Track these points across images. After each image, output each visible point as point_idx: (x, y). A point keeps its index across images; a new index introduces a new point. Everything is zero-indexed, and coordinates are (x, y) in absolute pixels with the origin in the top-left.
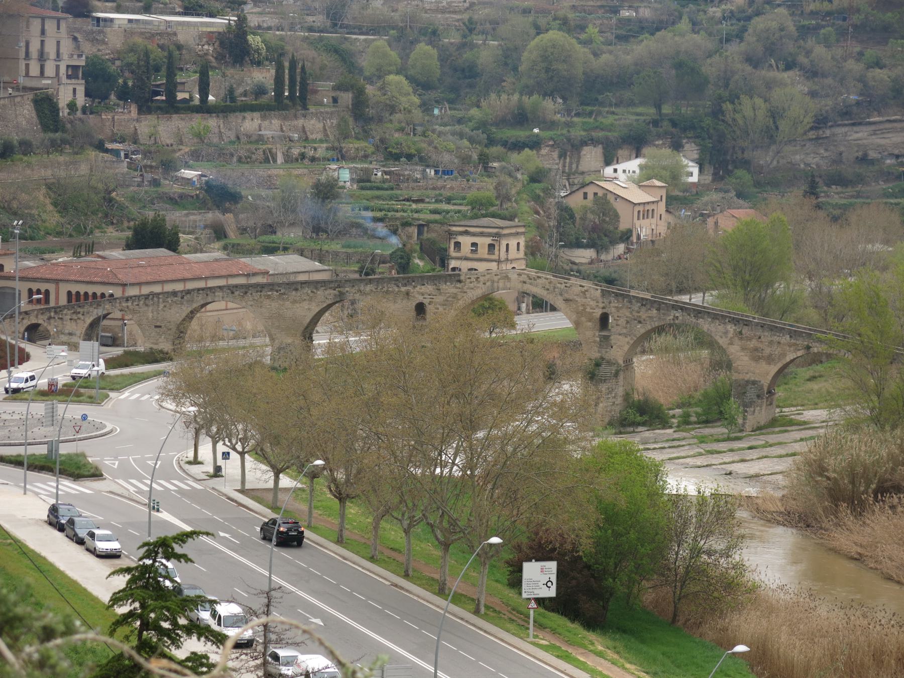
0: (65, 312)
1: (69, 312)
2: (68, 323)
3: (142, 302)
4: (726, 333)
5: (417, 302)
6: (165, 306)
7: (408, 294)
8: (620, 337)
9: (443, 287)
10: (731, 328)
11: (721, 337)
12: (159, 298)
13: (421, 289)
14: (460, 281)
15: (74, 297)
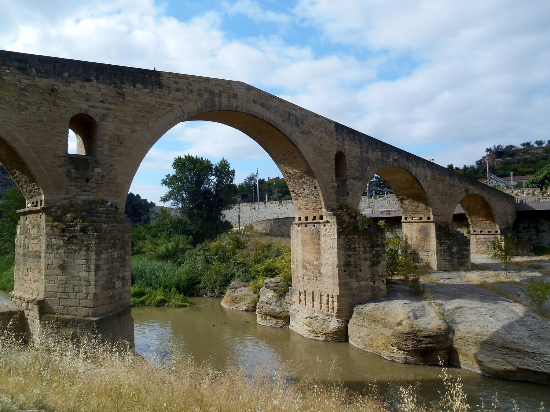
4: (426, 176)
5: (76, 112)
8: (355, 182)
9: (128, 89)
10: (428, 172)
11: (424, 182)
13: (81, 87)
14: (160, 86)
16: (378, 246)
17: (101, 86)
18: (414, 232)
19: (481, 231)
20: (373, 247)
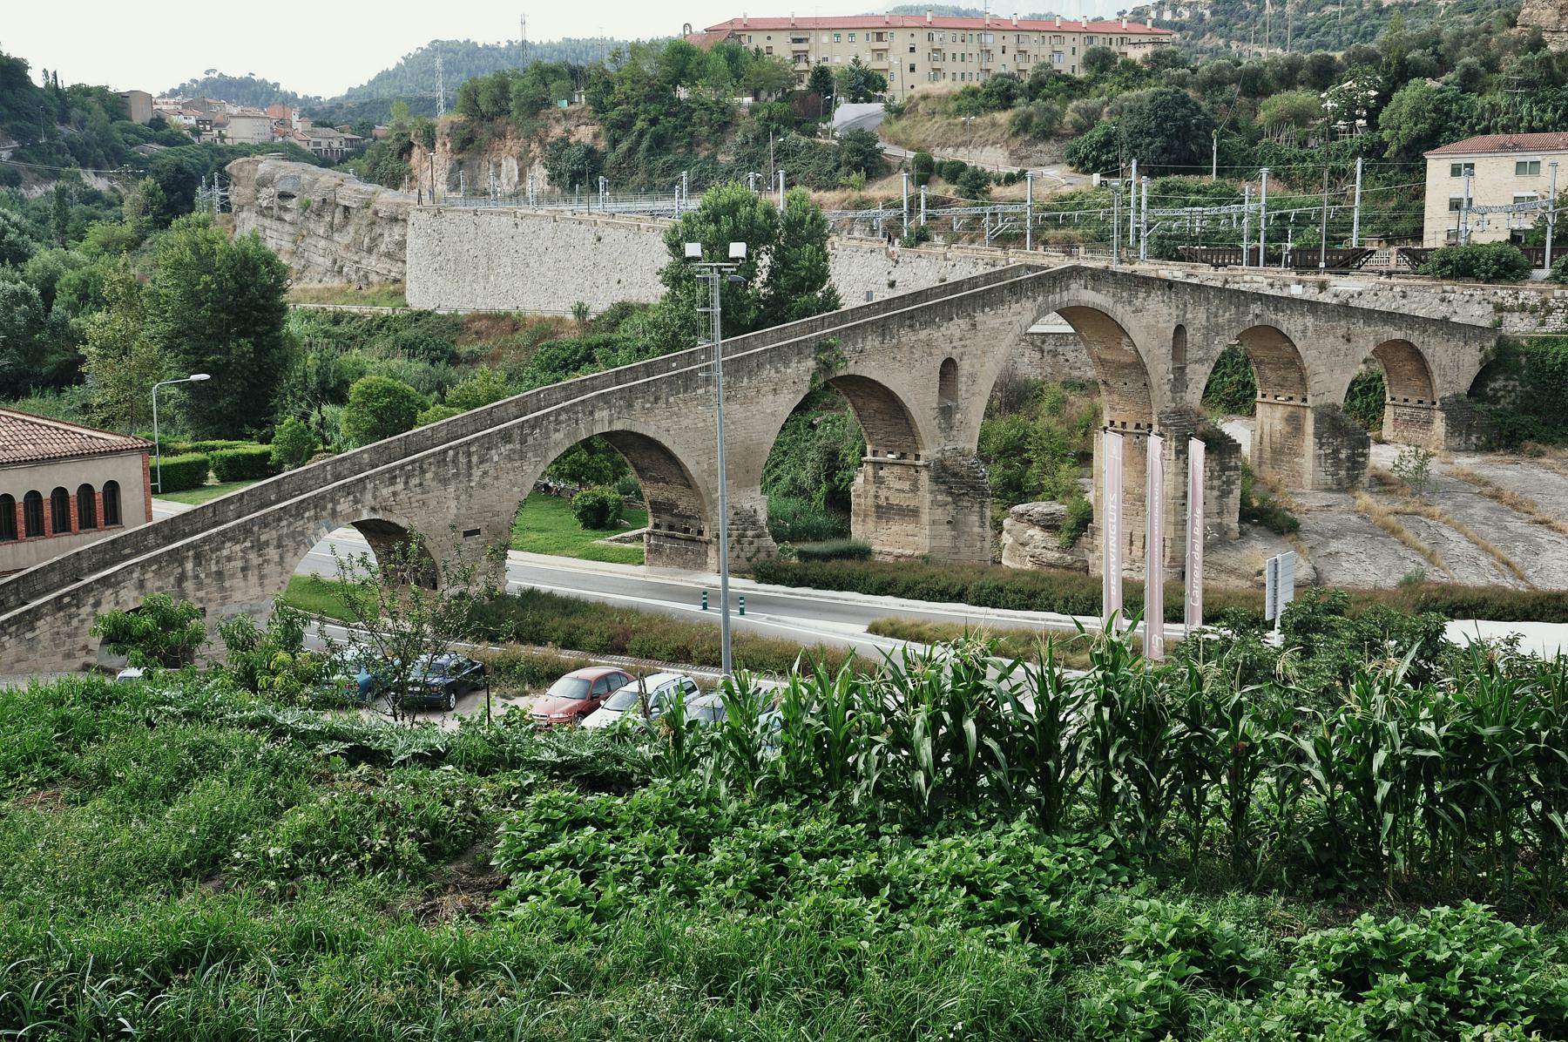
0: (225, 552)
1: (238, 548)
2: (238, 582)
3: (429, 475)
6: (485, 473)
7: (929, 344)
8: (1197, 366)
12: (469, 455)
15: (47, 511)
16: (1230, 469)
17: (961, 321)
18: (1276, 422)
19: (1406, 400)
20: (1224, 469)
